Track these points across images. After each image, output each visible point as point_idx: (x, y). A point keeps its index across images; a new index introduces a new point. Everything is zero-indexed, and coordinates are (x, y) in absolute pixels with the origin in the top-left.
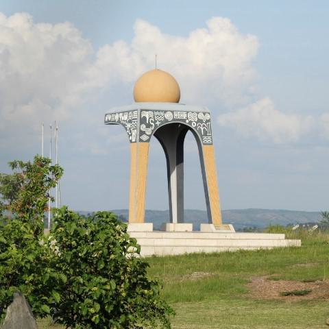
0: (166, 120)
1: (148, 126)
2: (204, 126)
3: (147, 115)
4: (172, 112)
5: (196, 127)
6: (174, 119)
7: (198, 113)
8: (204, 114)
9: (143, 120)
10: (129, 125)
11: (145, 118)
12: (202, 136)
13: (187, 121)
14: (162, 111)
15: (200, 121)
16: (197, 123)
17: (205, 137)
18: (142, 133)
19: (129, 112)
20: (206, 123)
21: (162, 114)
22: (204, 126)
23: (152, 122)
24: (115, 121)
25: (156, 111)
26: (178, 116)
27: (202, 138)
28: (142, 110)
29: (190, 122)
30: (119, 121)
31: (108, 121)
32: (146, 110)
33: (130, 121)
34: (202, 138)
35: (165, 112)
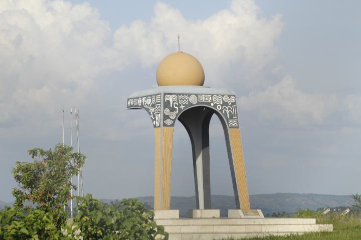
0: (191, 104)
2: (229, 109)
3: (171, 99)
4: (197, 95)
5: (221, 111)
7: (223, 96)
8: (230, 96)
9: (167, 104)
11: (168, 101)
12: (227, 119)
14: (186, 94)
15: (225, 104)
16: (222, 106)
17: (231, 121)
18: (166, 117)
19: (151, 96)
21: (186, 97)
22: (229, 109)
23: (176, 105)
24: (138, 106)
25: (180, 94)
26: (202, 99)
27: (228, 121)
28: (165, 94)
29: (215, 105)
33: (153, 106)
35: (190, 95)
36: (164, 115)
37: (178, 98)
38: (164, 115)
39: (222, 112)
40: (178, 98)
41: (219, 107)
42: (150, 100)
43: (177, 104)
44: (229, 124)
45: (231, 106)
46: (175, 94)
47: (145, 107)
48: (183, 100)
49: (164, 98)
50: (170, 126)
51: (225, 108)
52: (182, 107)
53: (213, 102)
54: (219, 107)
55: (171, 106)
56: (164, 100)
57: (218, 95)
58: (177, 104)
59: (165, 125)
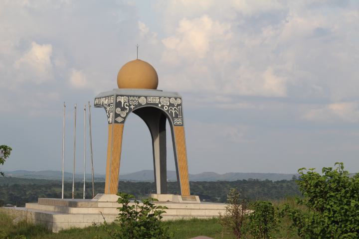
0: (140, 104)
1: (123, 109)
2: (175, 109)
3: (122, 100)
4: (146, 97)
5: (168, 111)
7: (170, 98)
8: (176, 99)
9: (118, 104)
10: (108, 109)
11: (120, 102)
14: (136, 97)
15: (171, 105)
16: (169, 106)
17: (176, 120)
18: (117, 115)
19: (108, 97)
20: (177, 107)
22: (175, 109)
23: (127, 105)
24: (100, 105)
25: (131, 96)
26: (151, 100)
27: (173, 120)
28: (117, 96)
29: (163, 106)
30: (103, 105)
31: (97, 105)
32: (122, 96)
33: (109, 105)
34: (173, 120)
35: (139, 97)
36: (116, 113)
37: (129, 99)
38: (116, 113)
40: (129, 99)
44: (174, 122)
45: (177, 107)
46: (126, 96)
47: (105, 106)
48: (134, 101)
49: (116, 99)
50: (120, 123)
51: (171, 109)
52: (132, 107)
53: (160, 103)
54: (166, 108)
56: (116, 100)
59: (116, 122)
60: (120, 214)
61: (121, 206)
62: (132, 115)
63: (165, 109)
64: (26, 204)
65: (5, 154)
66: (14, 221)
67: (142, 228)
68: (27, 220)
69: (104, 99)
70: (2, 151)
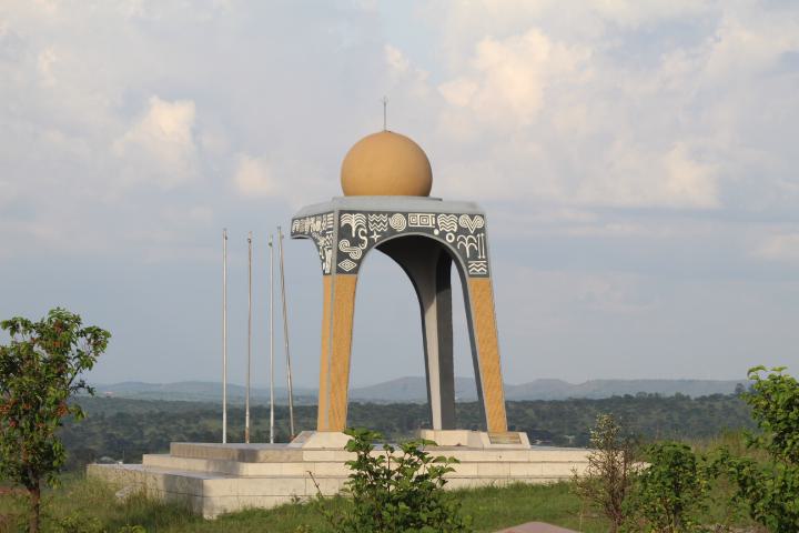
0: (392, 231)
1: (356, 242)
2: (471, 240)
3: (352, 221)
4: (405, 214)
5: (455, 244)
6: (408, 229)
7: (458, 216)
8: (472, 217)
9: (344, 232)
11: (348, 227)
12: (466, 260)
13: (436, 232)
14: (384, 213)
15: (462, 231)
16: (456, 234)
17: (473, 263)
18: (342, 256)
20: (475, 235)
21: (385, 218)
22: (471, 240)
23: (363, 234)
24: (303, 233)
25: (372, 213)
27: (467, 265)
28: (342, 212)
29: (443, 234)
30: (310, 234)
32: (351, 212)
33: (324, 234)
35: (391, 214)
36: (339, 252)
37: (367, 220)
38: (339, 252)
39: (456, 247)
40: (367, 220)
41: (450, 237)
42: (319, 223)
43: (366, 231)
44: (468, 269)
45: (475, 235)
46: (360, 212)
47: (315, 235)
48: (378, 223)
51: (462, 239)
52: (375, 237)
53: (437, 227)
54: (450, 237)
55: (354, 235)
57: (448, 215)
58: (366, 231)
59: (340, 271)
60: (352, 476)
61: (354, 457)
62: (375, 254)
63: (448, 241)
64: (145, 456)
65: (95, 345)
66: (118, 494)
67: (402, 506)
68: (145, 489)
69: (313, 219)
70: (89, 340)
